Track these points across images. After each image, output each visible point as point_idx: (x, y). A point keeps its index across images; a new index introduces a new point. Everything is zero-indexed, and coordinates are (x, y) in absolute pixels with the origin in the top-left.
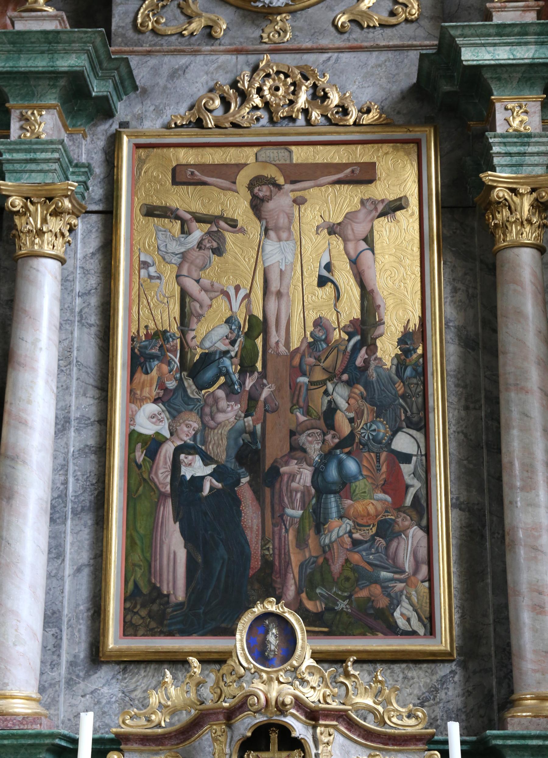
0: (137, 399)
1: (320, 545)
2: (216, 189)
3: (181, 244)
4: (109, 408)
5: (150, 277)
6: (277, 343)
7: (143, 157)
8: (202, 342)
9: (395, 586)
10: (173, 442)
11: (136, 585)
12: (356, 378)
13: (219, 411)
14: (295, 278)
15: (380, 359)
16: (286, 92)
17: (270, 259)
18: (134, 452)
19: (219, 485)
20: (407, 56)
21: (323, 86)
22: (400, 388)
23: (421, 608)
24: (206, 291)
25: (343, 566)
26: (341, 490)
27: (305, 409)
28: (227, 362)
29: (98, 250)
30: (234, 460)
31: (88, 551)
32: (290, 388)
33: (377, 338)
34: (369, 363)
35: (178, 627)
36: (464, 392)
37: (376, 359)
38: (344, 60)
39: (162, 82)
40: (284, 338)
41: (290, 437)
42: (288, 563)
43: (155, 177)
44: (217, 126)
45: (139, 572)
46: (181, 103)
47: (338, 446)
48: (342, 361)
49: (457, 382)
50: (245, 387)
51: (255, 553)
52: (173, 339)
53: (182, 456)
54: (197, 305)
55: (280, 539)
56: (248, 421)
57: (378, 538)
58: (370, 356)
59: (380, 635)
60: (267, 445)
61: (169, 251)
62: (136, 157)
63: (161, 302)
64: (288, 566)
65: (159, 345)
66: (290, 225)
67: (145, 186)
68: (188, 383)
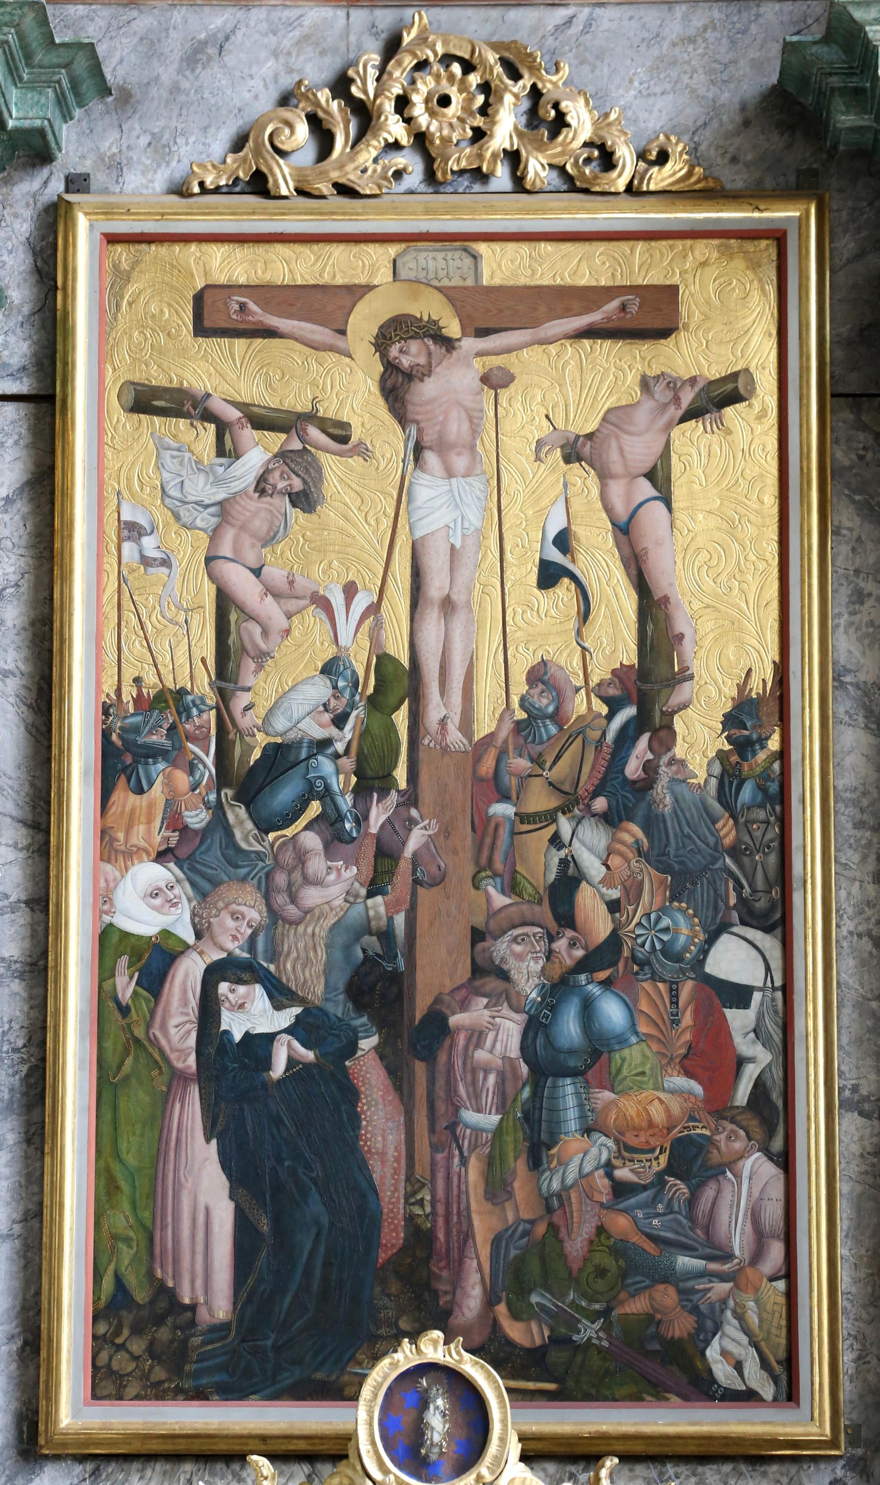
0: (116, 851)
1: (541, 1195)
2: (298, 346)
3: (218, 482)
4: (52, 874)
5: (146, 561)
6: (443, 722)
7: (125, 266)
8: (266, 719)
9: (709, 1289)
10: (201, 953)
11: (119, 1283)
12: (625, 807)
13: (307, 881)
14: (484, 566)
15: (682, 763)
16: (466, 108)
17: (425, 521)
18: (113, 975)
19: (309, 1055)
20: (758, 16)
21: (554, 96)
22: (727, 831)
23: (767, 1339)
24: (277, 596)
25: (591, 1242)
26: (589, 1067)
28: (326, 766)
29: (21, 490)
30: (342, 997)
31: (8, 1204)
32: (474, 829)
33: (675, 712)
34: (657, 773)
35: (217, 1378)
36: (875, 840)
37: (673, 761)
38: (605, 25)
39: (167, 74)
40: (459, 711)
41: (473, 944)
42: (467, 1235)
43: (153, 316)
44: (301, 192)
45: (126, 1254)
46: (212, 130)
47: (582, 966)
48: (593, 768)
49: (858, 816)
50: (368, 826)
51: (392, 1211)
52: (201, 712)
53: (224, 987)
54: (257, 630)
55: (448, 1178)
56: (375, 907)
57: (671, 1180)
58: (658, 756)
59: (674, 1399)
60: (419, 962)
61: (190, 498)
62: (108, 265)
63: (171, 621)
64: (465, 1241)
65: (166, 726)
66: (474, 439)
67: (131, 337)
68: (237, 816)
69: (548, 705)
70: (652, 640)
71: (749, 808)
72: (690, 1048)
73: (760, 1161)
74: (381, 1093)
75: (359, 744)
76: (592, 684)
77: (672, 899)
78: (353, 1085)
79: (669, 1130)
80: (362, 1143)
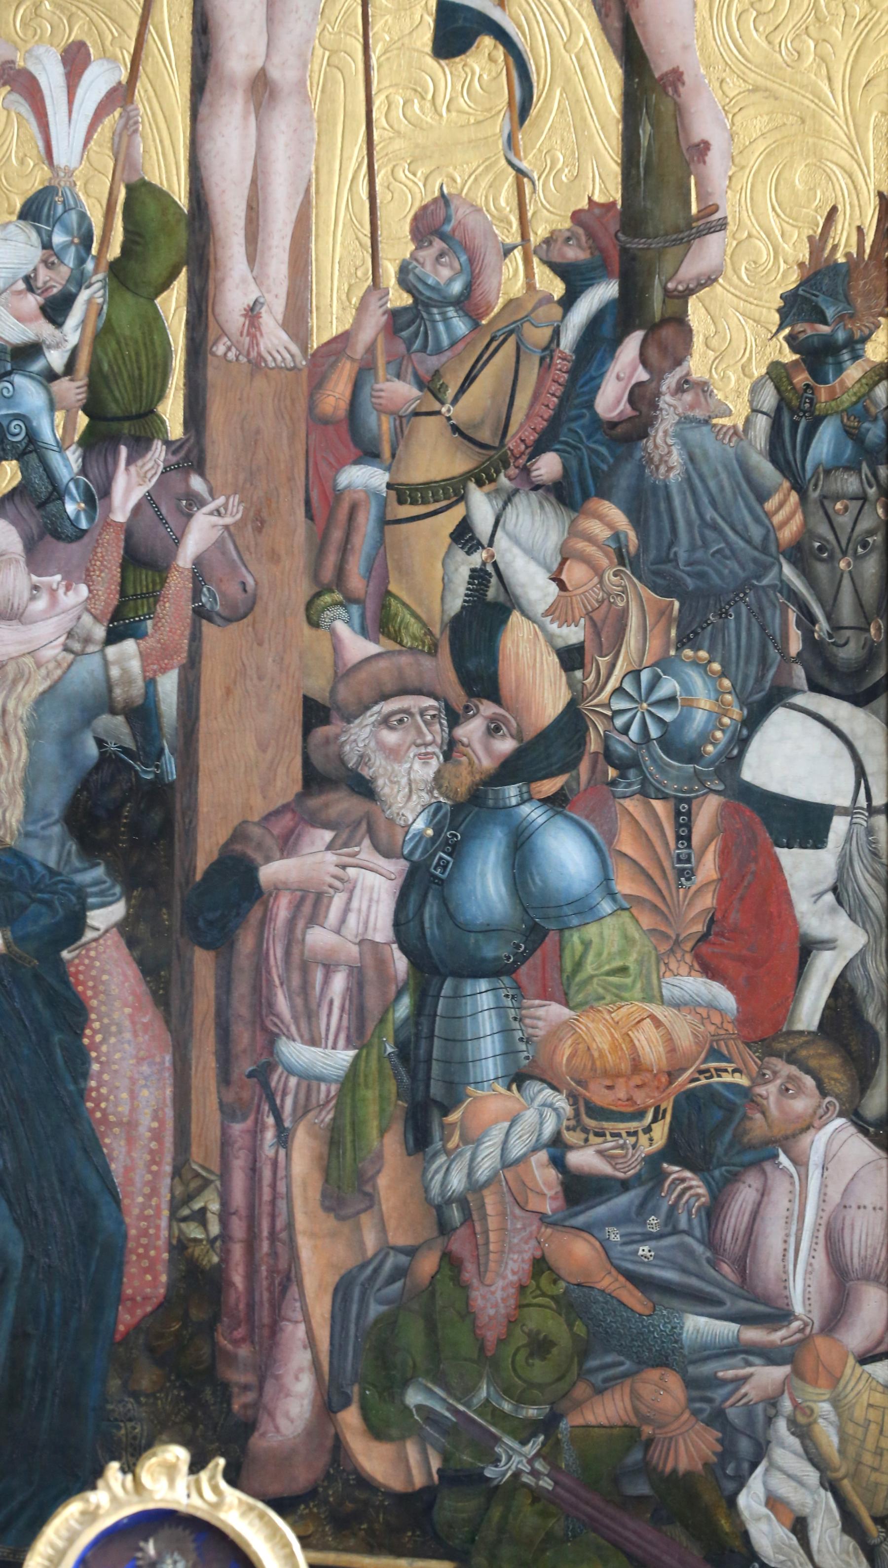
6: (252, 313)
12: (594, 470)
15: (703, 388)
26: (523, 958)
27: (371, 606)
32: (310, 515)
33: (690, 292)
34: (655, 407)
37: (685, 385)
40: (282, 290)
41: (307, 730)
48: (536, 397)
50: (109, 509)
56: (121, 660)
58: (657, 375)
69: (451, 280)
70: (649, 154)
71: (827, 472)
72: (712, 921)
73: (844, 1135)
74: (128, 1010)
75: (94, 354)
76: (534, 241)
77: (681, 644)
78: (76, 995)
79: (672, 1076)
80: (90, 1105)
